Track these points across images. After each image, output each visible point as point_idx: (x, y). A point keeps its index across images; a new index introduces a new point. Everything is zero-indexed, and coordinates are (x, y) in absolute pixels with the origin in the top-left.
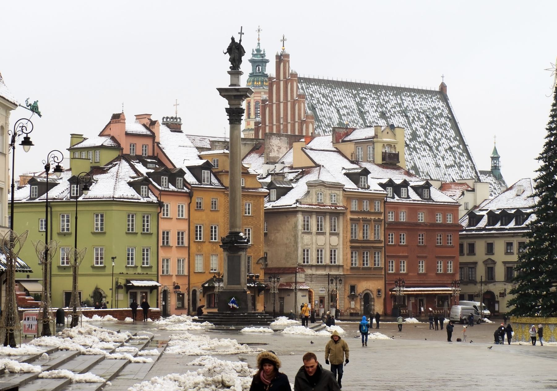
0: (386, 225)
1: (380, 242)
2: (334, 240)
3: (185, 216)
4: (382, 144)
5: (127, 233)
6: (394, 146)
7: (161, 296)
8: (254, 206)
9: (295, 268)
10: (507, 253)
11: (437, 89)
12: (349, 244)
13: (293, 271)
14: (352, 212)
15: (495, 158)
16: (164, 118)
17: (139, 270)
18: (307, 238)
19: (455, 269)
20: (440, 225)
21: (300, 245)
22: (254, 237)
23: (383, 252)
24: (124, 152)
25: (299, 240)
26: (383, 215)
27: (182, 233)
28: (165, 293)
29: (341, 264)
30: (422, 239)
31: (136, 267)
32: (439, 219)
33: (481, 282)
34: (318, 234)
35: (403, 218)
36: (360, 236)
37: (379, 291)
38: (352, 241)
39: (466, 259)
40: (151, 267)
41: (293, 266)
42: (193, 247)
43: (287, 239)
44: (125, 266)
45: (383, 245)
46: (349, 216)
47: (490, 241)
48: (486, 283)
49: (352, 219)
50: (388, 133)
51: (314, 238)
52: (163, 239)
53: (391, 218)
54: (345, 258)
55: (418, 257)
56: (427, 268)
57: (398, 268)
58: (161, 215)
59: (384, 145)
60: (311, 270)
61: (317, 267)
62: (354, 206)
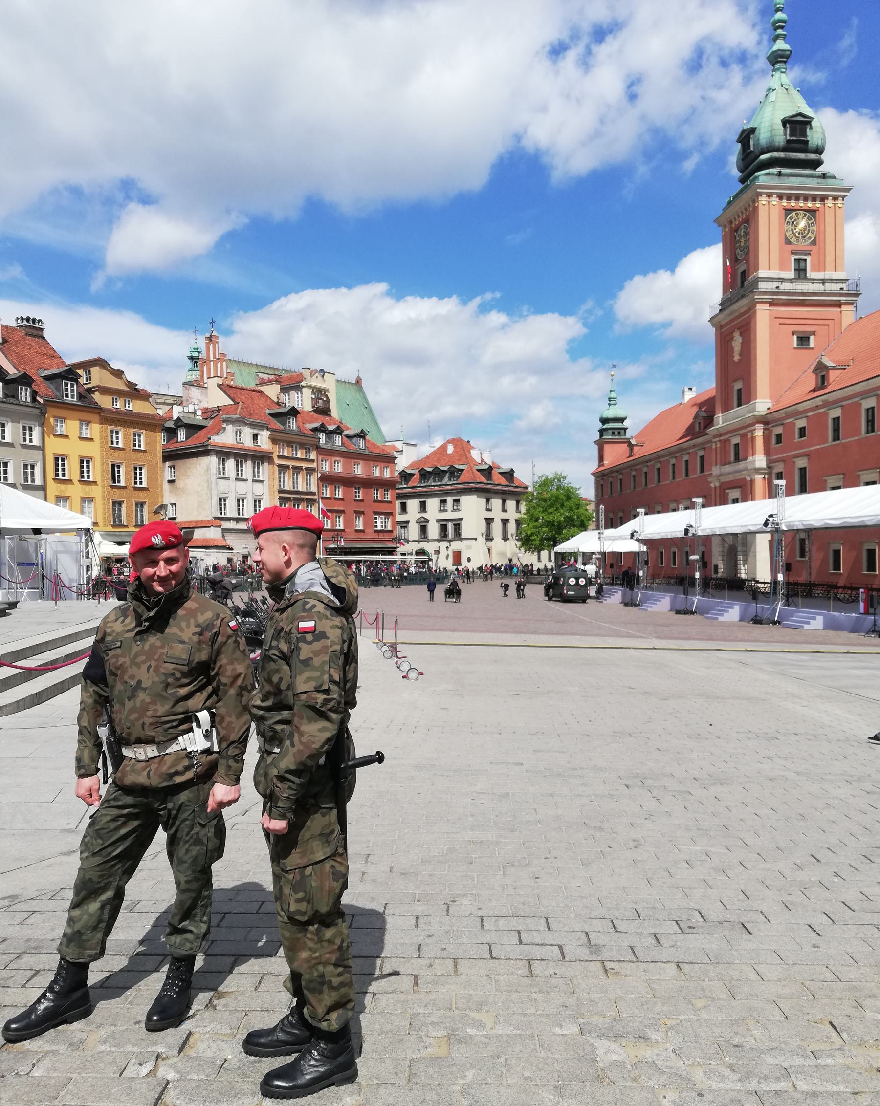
1: (314, 494)
2: (259, 489)
3: (36, 442)
10: (441, 511)
12: (277, 494)
14: (280, 457)
16: (18, 319)
19: (393, 526)
21: (214, 492)
22: (148, 478)
27: (33, 467)
32: (376, 472)
33: (414, 541)
36: (288, 486)
38: (280, 491)
43: (199, 485)
48: (418, 541)
49: (279, 466)
51: (232, 483)
53: (326, 467)
55: (356, 512)
56: (365, 524)
61: (237, 520)
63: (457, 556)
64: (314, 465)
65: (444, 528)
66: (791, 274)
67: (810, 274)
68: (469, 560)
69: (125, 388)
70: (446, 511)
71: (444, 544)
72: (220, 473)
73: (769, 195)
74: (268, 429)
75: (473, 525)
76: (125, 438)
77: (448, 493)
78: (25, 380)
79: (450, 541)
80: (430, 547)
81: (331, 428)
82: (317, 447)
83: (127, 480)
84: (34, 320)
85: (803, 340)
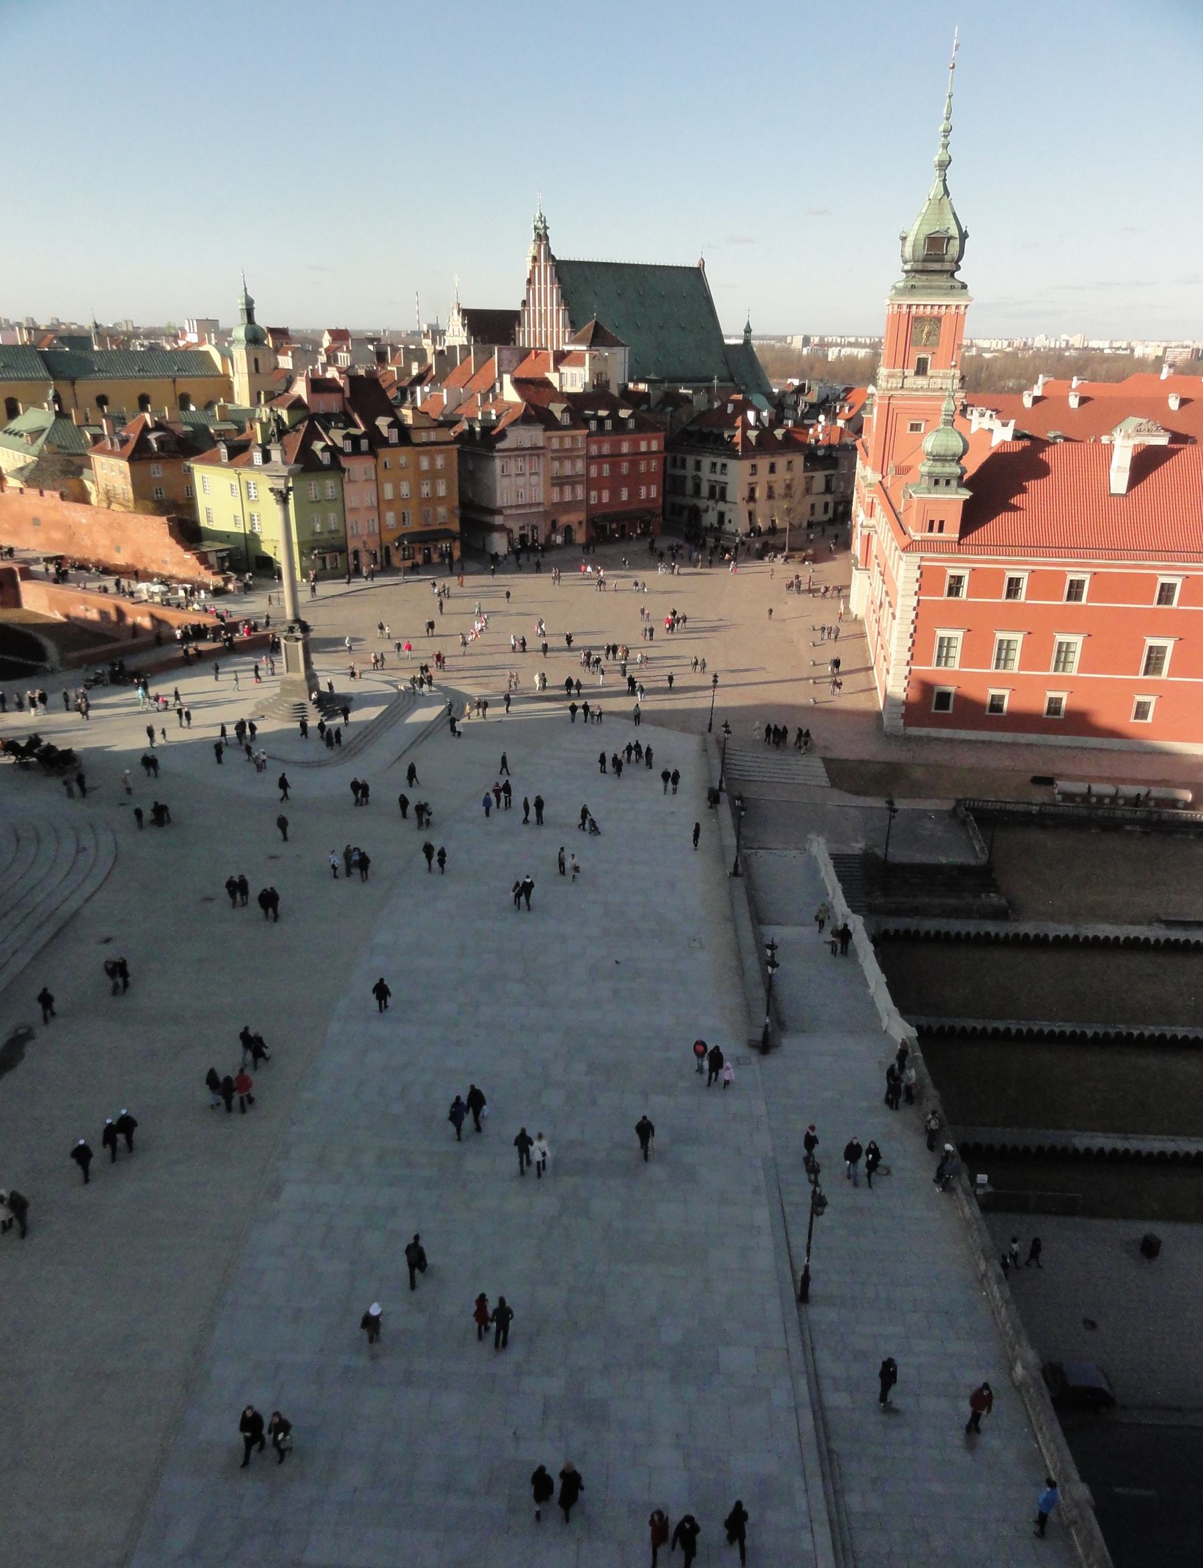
2: (534, 479)
7: (351, 557)
11: (696, 266)
15: (748, 330)
17: (326, 536)
18: (506, 481)
20: (645, 453)
25: (498, 484)
28: (356, 554)
30: (625, 468)
32: (643, 447)
34: (517, 475)
35: (606, 449)
37: (580, 523)
39: (679, 472)
46: (550, 455)
47: (699, 458)
48: (692, 497)
53: (594, 450)
57: (600, 498)
58: (346, 479)
63: (721, 516)
65: (712, 488)
66: (910, 372)
67: (930, 372)
68: (730, 521)
70: (715, 472)
71: (711, 503)
73: (900, 306)
74: (545, 430)
75: (737, 492)
77: (719, 455)
78: (364, 435)
79: (717, 502)
80: (702, 504)
81: (603, 413)
82: (589, 435)
85: (915, 427)
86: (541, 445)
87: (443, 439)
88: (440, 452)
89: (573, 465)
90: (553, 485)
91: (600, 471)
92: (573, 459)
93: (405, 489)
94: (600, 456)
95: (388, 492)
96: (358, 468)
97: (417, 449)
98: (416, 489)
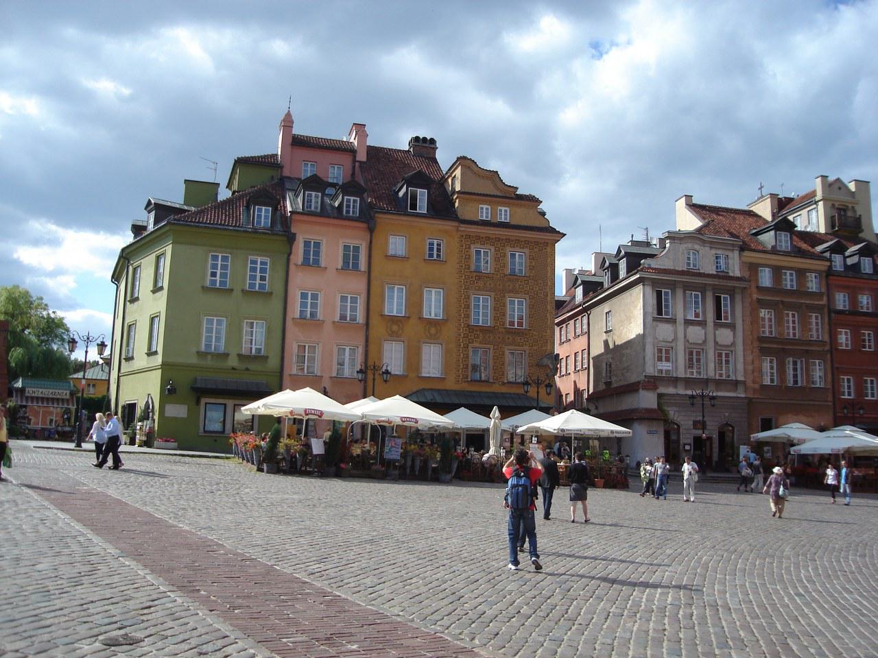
0: (833, 315)
1: (822, 343)
2: (725, 336)
3: (363, 266)
4: (830, 204)
5: (204, 289)
6: (853, 207)
8: (532, 258)
9: (639, 382)
12: (756, 344)
13: (633, 388)
17: (233, 362)
23: (829, 362)
24: (286, 173)
26: (825, 298)
27: (354, 300)
29: (741, 378)
31: (225, 356)
34: (688, 323)
38: (762, 340)
40: (266, 358)
41: (639, 379)
42: (378, 328)
44: (194, 350)
45: (827, 348)
46: (755, 296)
49: (759, 300)
50: (840, 188)
52: (304, 305)
54: (750, 368)
59: (833, 205)
60: (676, 387)
62: (766, 279)
64: (824, 301)
69: (501, 195)
72: (660, 312)
76: (497, 260)
83: (495, 319)
84: (425, 139)
86: (738, 274)
87: (525, 224)
88: (518, 243)
89: (805, 323)
90: (764, 352)
91: (857, 340)
92: (803, 311)
93: (433, 305)
94: (854, 312)
95: (395, 304)
96: (333, 243)
97: (463, 227)
98: (459, 306)
